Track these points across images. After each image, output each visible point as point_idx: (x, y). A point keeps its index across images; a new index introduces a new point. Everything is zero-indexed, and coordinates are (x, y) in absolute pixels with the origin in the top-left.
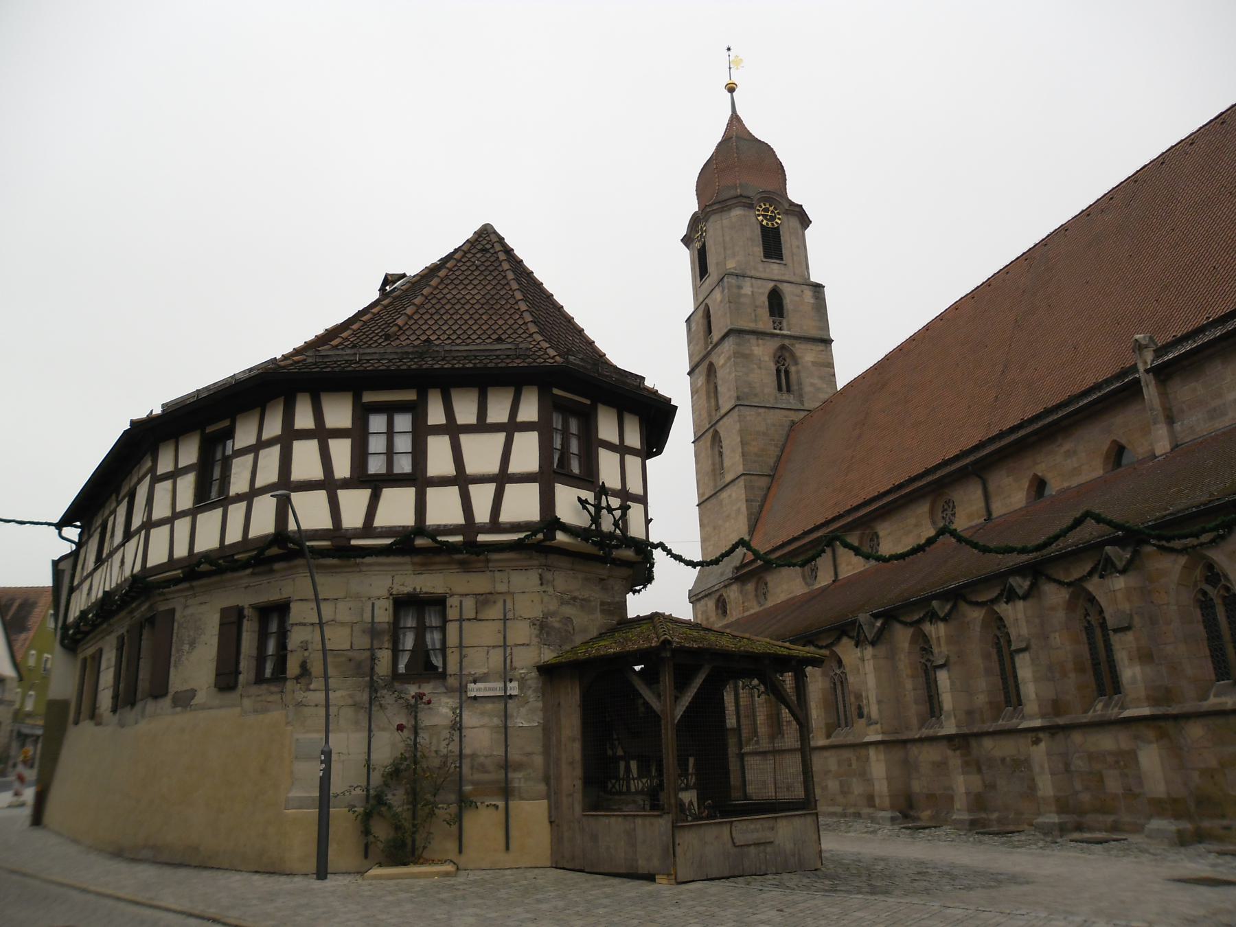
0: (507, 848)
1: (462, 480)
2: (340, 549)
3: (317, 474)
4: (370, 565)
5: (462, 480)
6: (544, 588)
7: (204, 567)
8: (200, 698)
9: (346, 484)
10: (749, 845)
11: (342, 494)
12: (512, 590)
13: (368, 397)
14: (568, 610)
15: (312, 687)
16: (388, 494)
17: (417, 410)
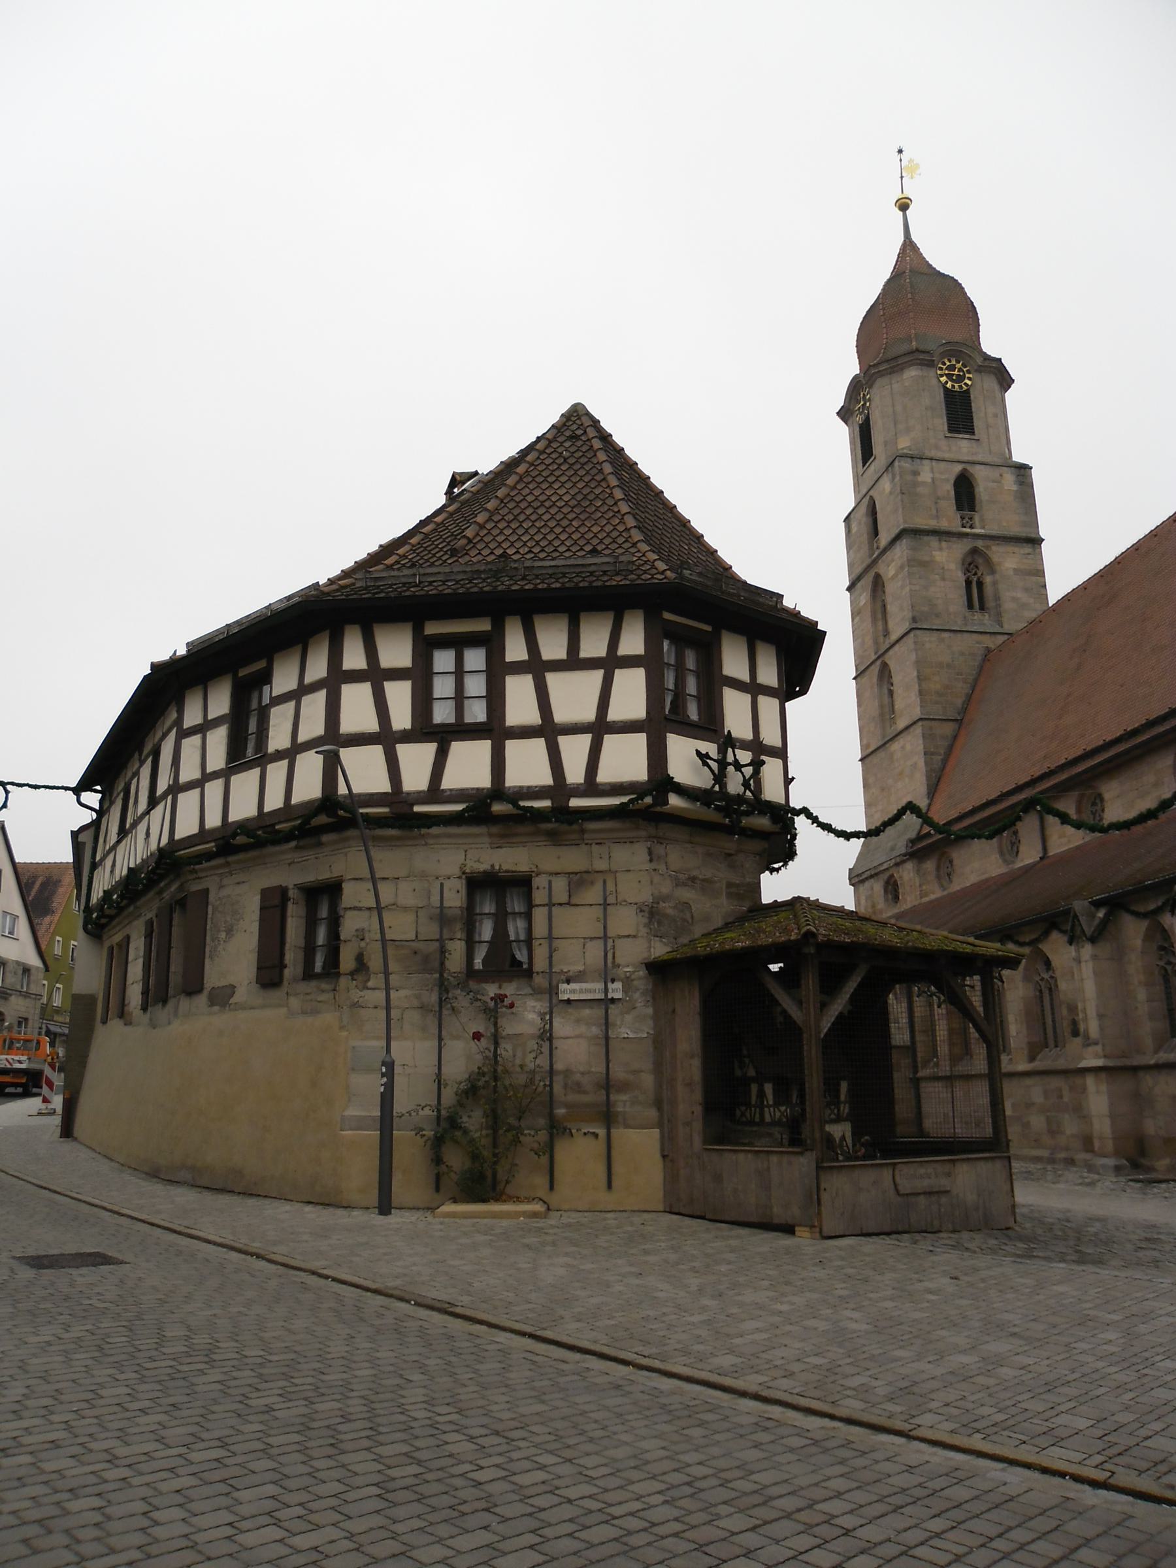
0: (610, 1186)
1: (549, 730)
2: (401, 816)
3: (371, 724)
4: (437, 836)
5: (549, 730)
6: (654, 865)
7: (241, 840)
8: (240, 996)
9: (407, 737)
10: (919, 1194)
11: (402, 750)
12: (614, 868)
13: (432, 629)
14: (686, 894)
15: (370, 984)
16: (458, 749)
17: (493, 643)
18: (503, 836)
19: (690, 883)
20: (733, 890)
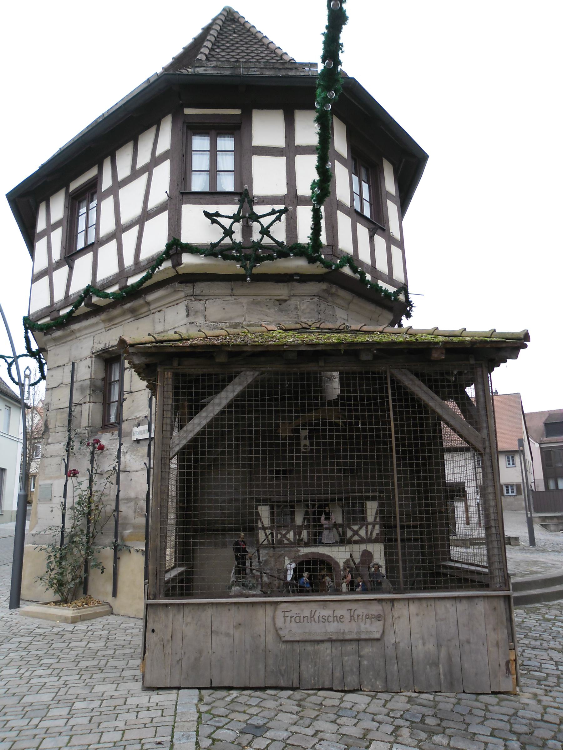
4: (80, 330)
6: (191, 319)
10: (322, 641)
15: (50, 441)
18: (111, 320)
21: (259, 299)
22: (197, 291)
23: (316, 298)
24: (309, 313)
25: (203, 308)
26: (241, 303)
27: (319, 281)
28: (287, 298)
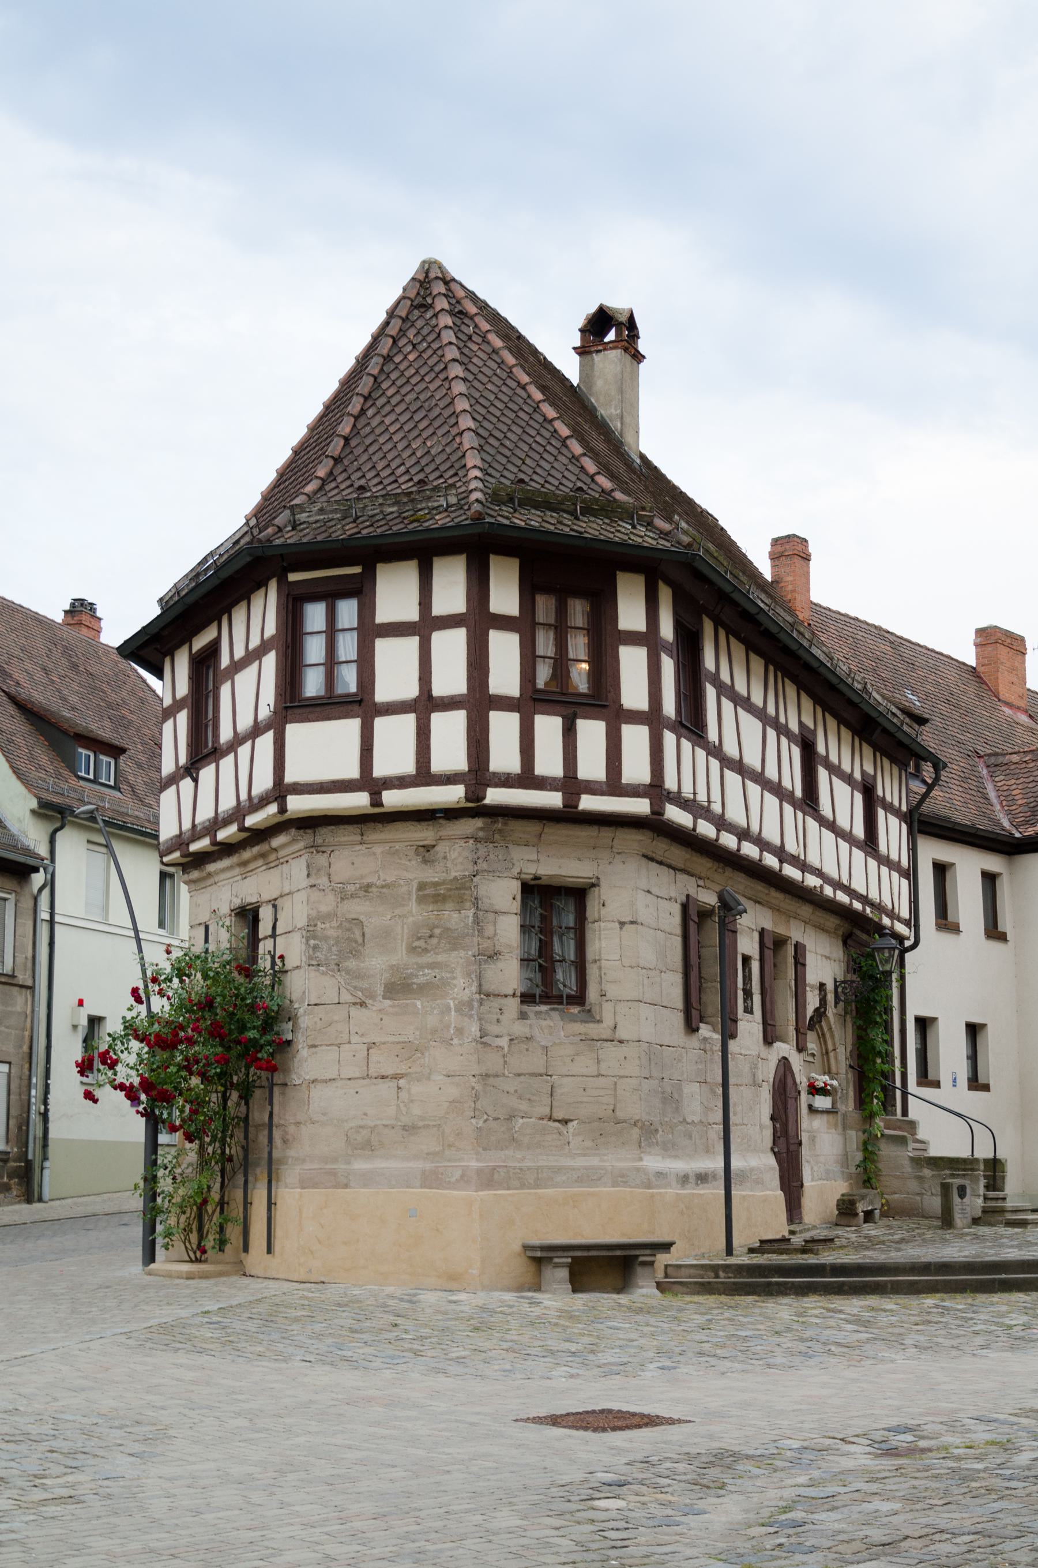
0: (269, 1251)
6: (312, 881)
14: (355, 908)
19: (362, 893)
20: (430, 891)
21: (397, 846)
22: (319, 841)
23: (471, 841)
24: (462, 863)
25: (327, 864)
26: (374, 854)
27: (473, 817)
28: (434, 843)
